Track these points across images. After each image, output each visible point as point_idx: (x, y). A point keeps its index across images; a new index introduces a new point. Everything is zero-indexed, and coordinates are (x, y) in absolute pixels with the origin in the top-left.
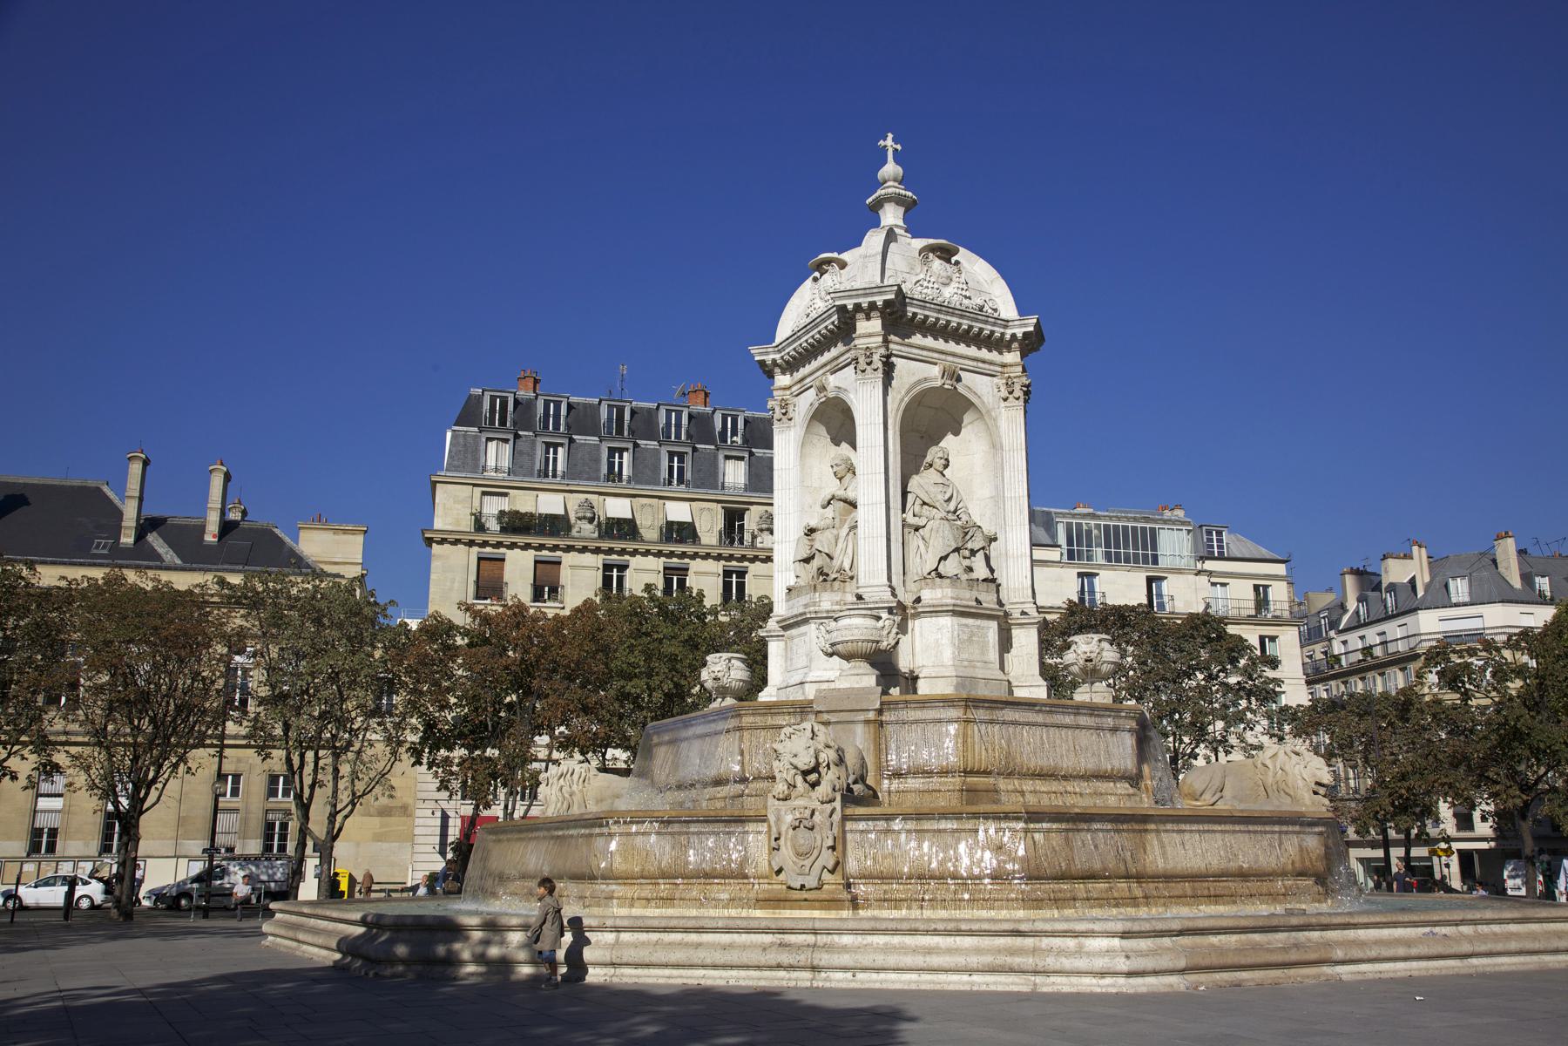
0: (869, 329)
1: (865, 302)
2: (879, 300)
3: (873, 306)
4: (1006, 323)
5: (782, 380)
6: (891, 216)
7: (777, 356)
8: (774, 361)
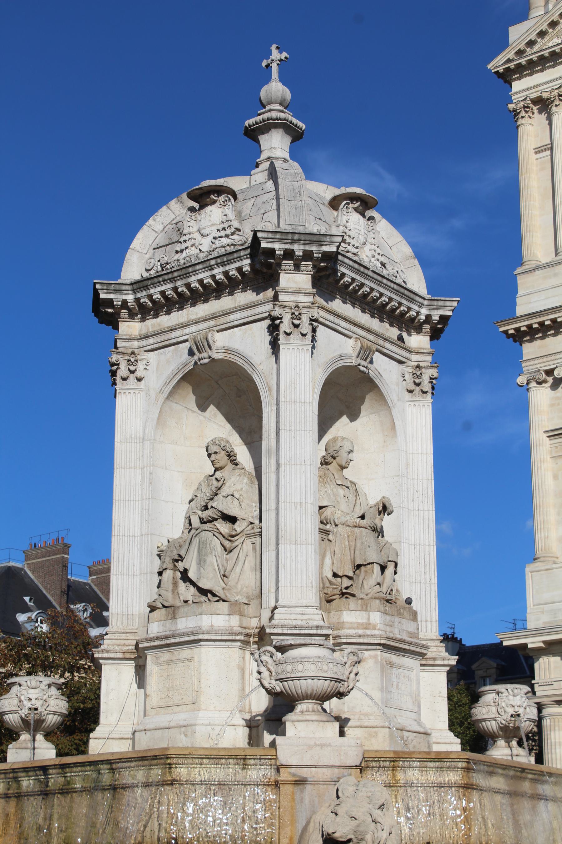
0: (295, 282)
1: (299, 249)
3: (308, 256)
4: (411, 296)
5: (129, 328)
6: (275, 144)
7: (130, 297)
8: (125, 303)
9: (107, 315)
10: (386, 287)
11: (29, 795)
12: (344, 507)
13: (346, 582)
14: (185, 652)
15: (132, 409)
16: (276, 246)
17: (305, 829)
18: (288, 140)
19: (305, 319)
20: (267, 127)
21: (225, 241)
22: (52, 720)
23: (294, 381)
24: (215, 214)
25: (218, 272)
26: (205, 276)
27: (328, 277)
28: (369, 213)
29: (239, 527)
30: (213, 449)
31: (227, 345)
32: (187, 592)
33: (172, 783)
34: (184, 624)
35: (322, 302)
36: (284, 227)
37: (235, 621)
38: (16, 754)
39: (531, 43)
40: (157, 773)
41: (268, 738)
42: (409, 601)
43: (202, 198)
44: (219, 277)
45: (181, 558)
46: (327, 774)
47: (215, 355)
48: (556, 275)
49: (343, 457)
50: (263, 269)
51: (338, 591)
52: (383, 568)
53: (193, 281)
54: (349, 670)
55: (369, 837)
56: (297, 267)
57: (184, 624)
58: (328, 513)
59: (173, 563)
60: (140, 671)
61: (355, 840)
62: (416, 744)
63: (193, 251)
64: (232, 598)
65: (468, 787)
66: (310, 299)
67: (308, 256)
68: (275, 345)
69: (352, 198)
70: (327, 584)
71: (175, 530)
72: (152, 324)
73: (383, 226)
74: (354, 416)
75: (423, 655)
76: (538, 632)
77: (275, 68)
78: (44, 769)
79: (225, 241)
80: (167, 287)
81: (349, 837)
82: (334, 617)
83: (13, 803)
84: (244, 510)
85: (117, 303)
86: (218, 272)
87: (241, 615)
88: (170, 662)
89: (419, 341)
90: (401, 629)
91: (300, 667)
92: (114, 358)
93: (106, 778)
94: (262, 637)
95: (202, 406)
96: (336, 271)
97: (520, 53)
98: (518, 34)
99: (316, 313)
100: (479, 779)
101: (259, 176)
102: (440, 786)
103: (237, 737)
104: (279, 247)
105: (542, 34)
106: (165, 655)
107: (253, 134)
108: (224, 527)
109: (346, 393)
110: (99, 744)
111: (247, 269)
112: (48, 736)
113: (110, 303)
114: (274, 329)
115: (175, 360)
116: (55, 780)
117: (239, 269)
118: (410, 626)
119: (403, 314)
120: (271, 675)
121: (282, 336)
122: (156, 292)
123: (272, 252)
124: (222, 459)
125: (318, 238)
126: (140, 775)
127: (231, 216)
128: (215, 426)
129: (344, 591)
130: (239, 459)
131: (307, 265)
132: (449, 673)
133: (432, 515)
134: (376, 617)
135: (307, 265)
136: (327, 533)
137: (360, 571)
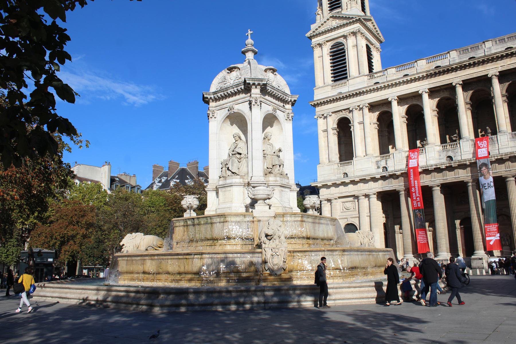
0: (256, 91)
1: (256, 83)
2: (261, 83)
3: (259, 84)
4: (286, 95)
5: (212, 104)
6: (250, 56)
7: (212, 96)
8: (211, 98)
9: (206, 101)
10: (280, 92)
11: (189, 225)
12: (269, 150)
13: (270, 170)
14: (229, 189)
15: (214, 125)
16: (250, 82)
17: (260, 233)
18: (253, 54)
19: (258, 101)
20: (247, 51)
21: (237, 81)
22: (195, 206)
23: (255, 117)
24: (234, 74)
25: (235, 89)
26: (232, 90)
27: (264, 90)
28: (275, 73)
29: (242, 156)
30: (235, 136)
31: (238, 108)
32: (229, 173)
33: (226, 222)
34: (228, 181)
35: (263, 96)
36: (252, 77)
37: (241, 180)
38: (186, 215)
39: (317, 29)
40: (222, 219)
41: (250, 210)
42: (287, 174)
43: (231, 70)
44: (236, 90)
45: (227, 164)
46: (266, 219)
47: (235, 111)
49: (269, 138)
50: (247, 88)
51: (268, 172)
52: (280, 166)
53: (229, 92)
55: (277, 234)
56: (256, 87)
57: (228, 181)
58: (265, 152)
59: (225, 166)
60: (217, 193)
62: (289, 211)
63: (229, 84)
64: (241, 175)
65: (302, 221)
66: (260, 96)
67: (259, 84)
68: (250, 108)
69: (270, 69)
71: (226, 157)
72: (218, 103)
73: (279, 76)
74: (272, 126)
75: (290, 188)
76: (321, 182)
77: (249, 35)
78: (193, 219)
79: (237, 81)
80: (222, 93)
82: (267, 179)
83: (186, 227)
84: (243, 151)
85: (209, 98)
86: (235, 89)
87: (243, 179)
88: (225, 191)
89: (289, 106)
90: (285, 182)
92: (208, 112)
93: (209, 221)
94: (249, 184)
95: (232, 125)
96: (266, 88)
97: (314, 32)
98: (313, 27)
99: (262, 99)
100: (305, 219)
101: (246, 64)
103: (243, 210)
104: (251, 82)
105: (319, 27)
106: (224, 189)
107: (244, 53)
108: (238, 156)
109: (269, 120)
110: (208, 212)
111: (243, 88)
112: (194, 211)
113: (207, 98)
114: (250, 104)
115: (225, 113)
116: (196, 221)
117: (241, 88)
118: (287, 181)
119: (284, 100)
121: (252, 106)
122: (219, 95)
123: (249, 83)
124: (237, 138)
125: (261, 80)
126: (218, 220)
127: (239, 74)
128: (235, 130)
130: (242, 138)
131: (259, 87)
132: (297, 193)
133: (292, 152)
134: (278, 179)
135: (259, 87)
136: (265, 157)
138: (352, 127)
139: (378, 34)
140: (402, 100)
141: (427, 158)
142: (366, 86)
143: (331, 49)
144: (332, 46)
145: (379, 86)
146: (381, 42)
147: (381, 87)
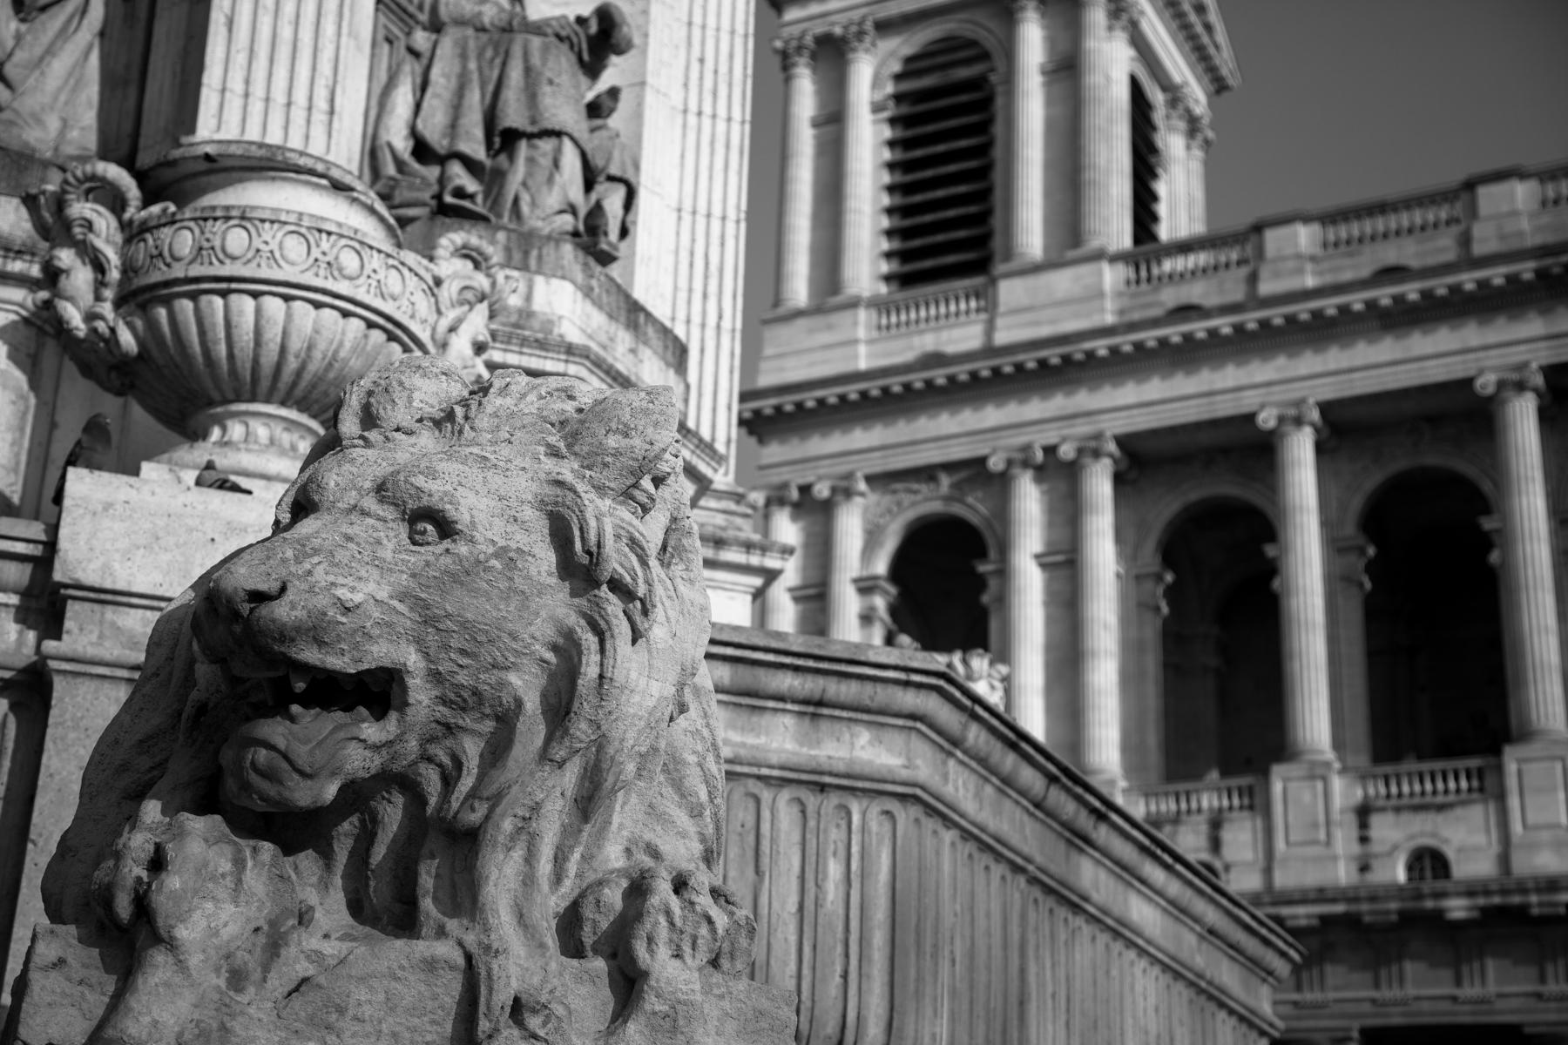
48: (830, 327)
54: (451, 315)
61: (420, 694)
70: (390, 169)
81: (380, 653)
91: (236, 240)
102: (816, 782)
120: (100, 284)
129: (448, 199)
137: (512, 159)
138: (993, 583)
139: (1208, 27)
140: (1343, 428)
141: (1517, 827)
142: (1109, 319)
143: (898, 78)
144: (909, 60)
145: (1199, 328)
146: (1219, 86)
147: (1213, 333)
